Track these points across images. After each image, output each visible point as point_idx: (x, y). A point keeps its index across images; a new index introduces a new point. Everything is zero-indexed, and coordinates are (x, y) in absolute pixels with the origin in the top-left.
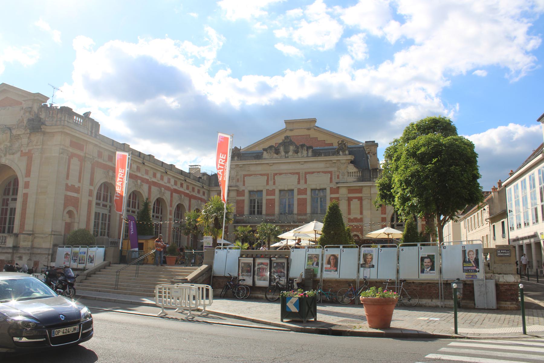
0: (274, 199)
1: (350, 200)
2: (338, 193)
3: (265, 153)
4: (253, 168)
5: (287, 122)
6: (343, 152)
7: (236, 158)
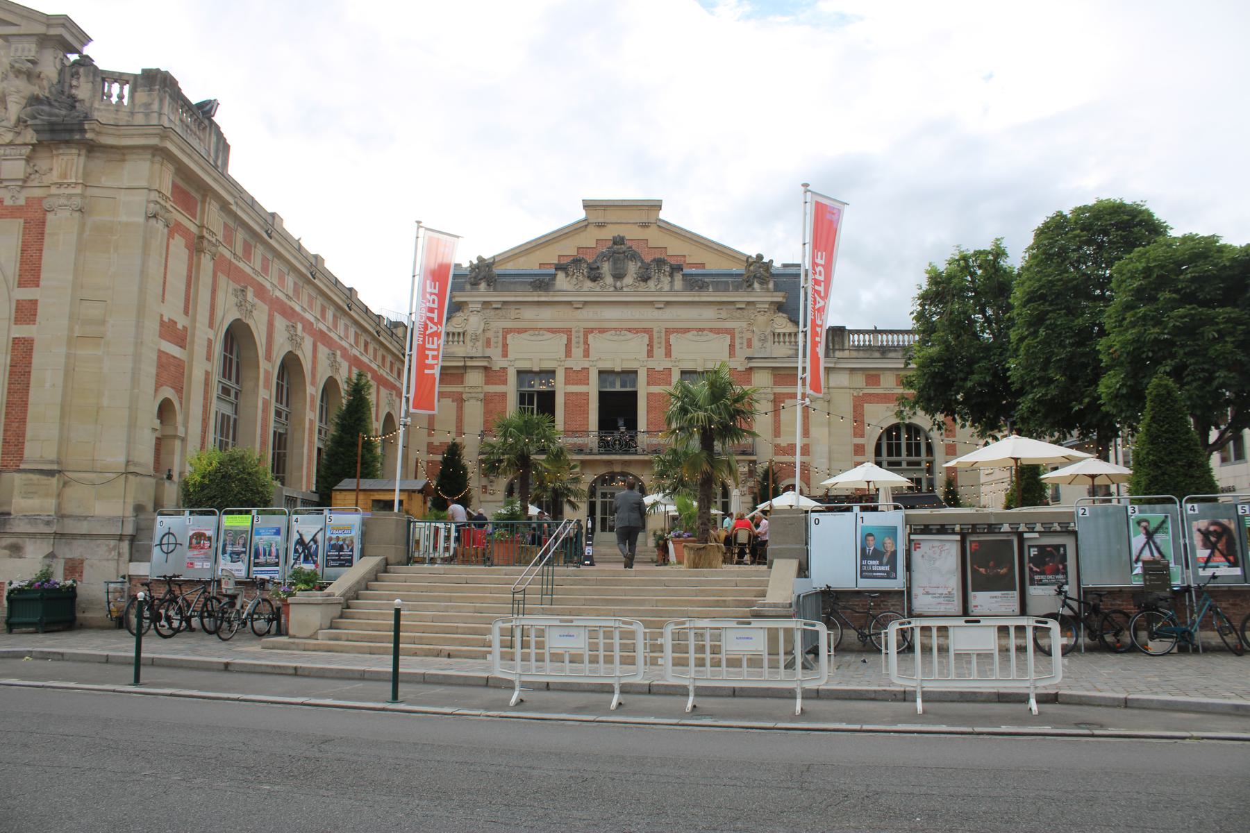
0: (587, 394)
1: (777, 400)
2: (749, 382)
3: (561, 276)
4: (528, 313)
5: (589, 206)
6: (761, 283)
7: (483, 286)
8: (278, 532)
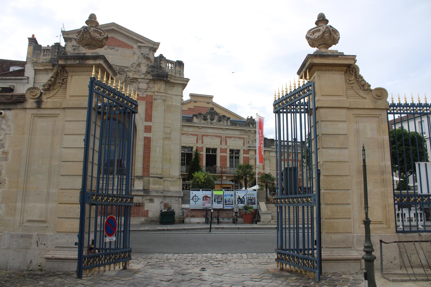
8: (232, 196)
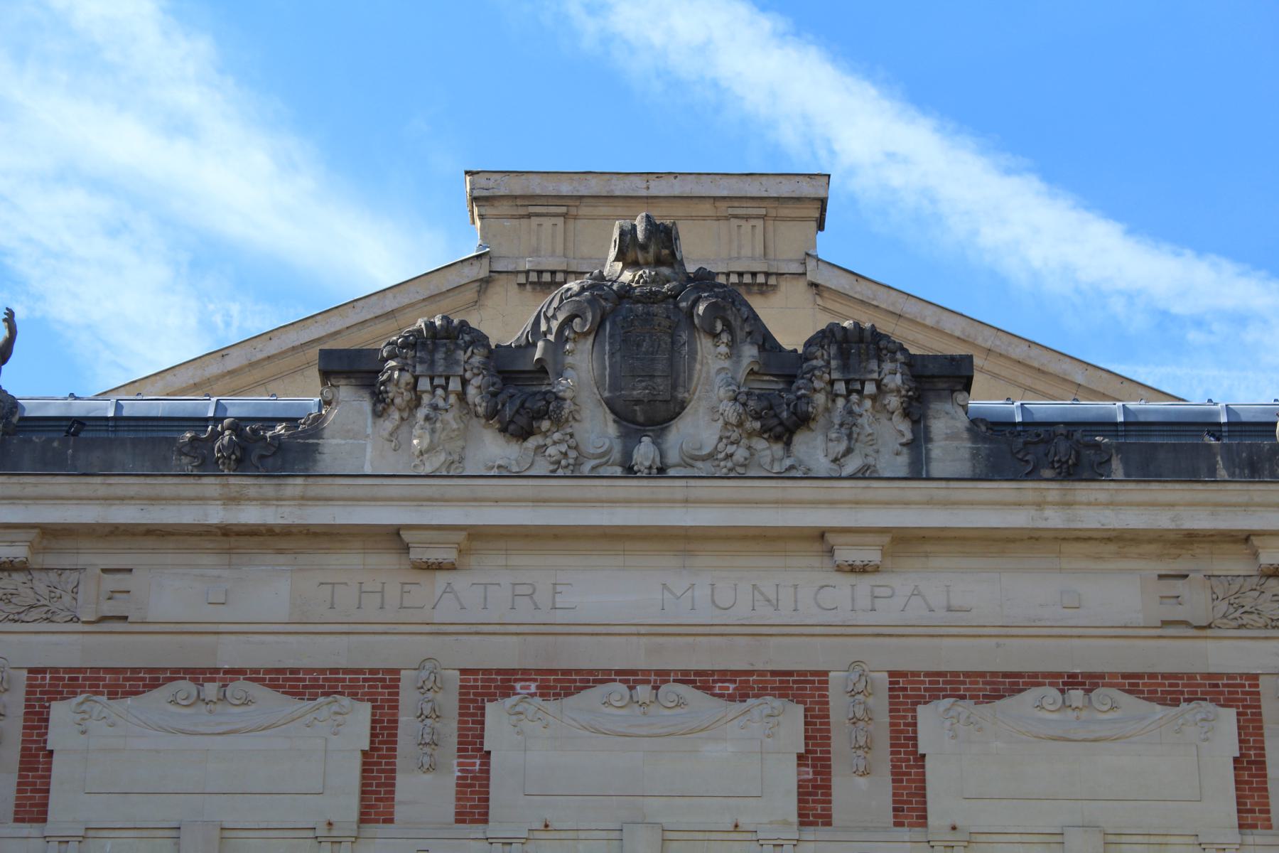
3: (351, 405)
4: (173, 594)
